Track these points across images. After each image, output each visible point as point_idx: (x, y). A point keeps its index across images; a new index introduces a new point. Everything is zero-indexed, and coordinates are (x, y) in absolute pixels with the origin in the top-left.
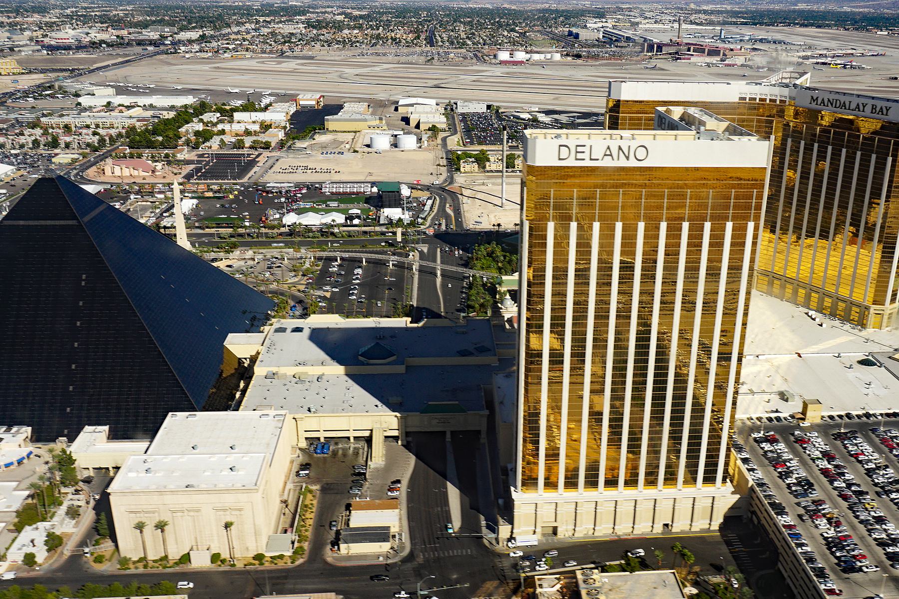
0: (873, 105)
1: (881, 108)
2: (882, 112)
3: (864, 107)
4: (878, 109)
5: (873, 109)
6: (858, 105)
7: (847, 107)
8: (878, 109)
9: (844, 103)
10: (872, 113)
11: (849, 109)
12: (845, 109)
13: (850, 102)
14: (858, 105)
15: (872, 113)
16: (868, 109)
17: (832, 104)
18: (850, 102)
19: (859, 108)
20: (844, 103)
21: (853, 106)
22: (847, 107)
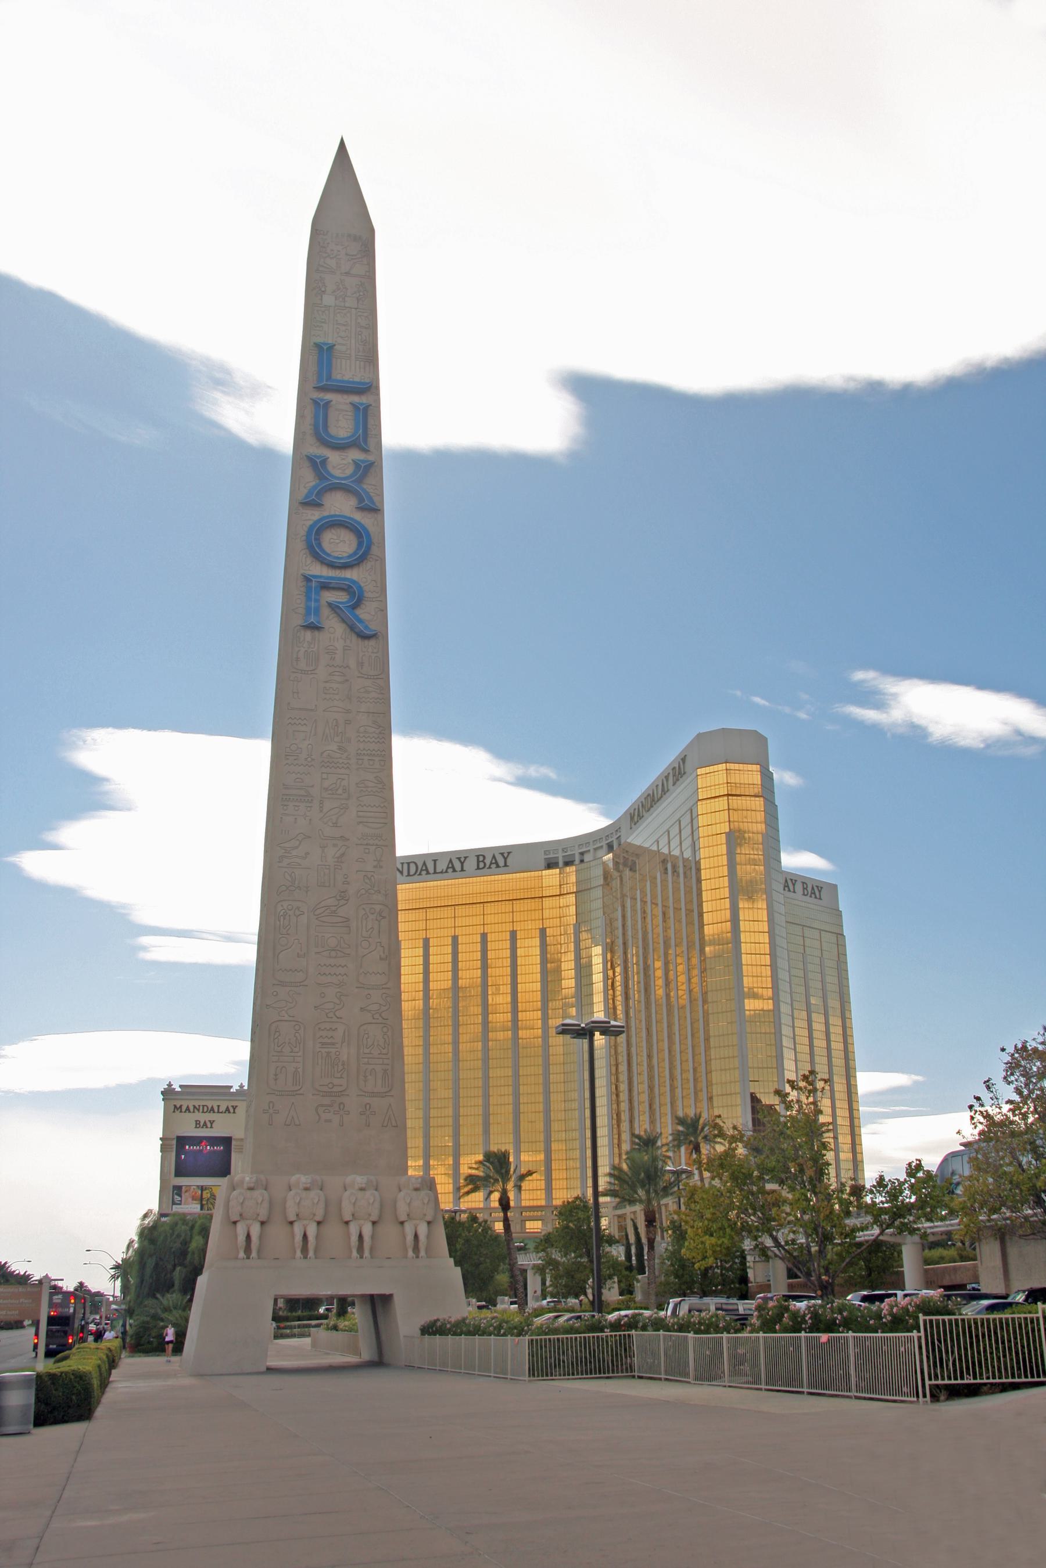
0: (478, 856)
1: (494, 857)
2: (496, 863)
3: (462, 863)
4: (202, 1124)
5: (196, 1124)
6: (451, 861)
7: (431, 870)
8: (202, 1124)
9: (424, 864)
10: (478, 868)
11: (435, 872)
12: (428, 873)
13: (435, 861)
14: (451, 861)
15: (478, 868)
16: (471, 864)
17: (401, 873)
18: (435, 861)
19: (453, 867)
20: (424, 864)
21: (442, 866)
22: (431, 870)
